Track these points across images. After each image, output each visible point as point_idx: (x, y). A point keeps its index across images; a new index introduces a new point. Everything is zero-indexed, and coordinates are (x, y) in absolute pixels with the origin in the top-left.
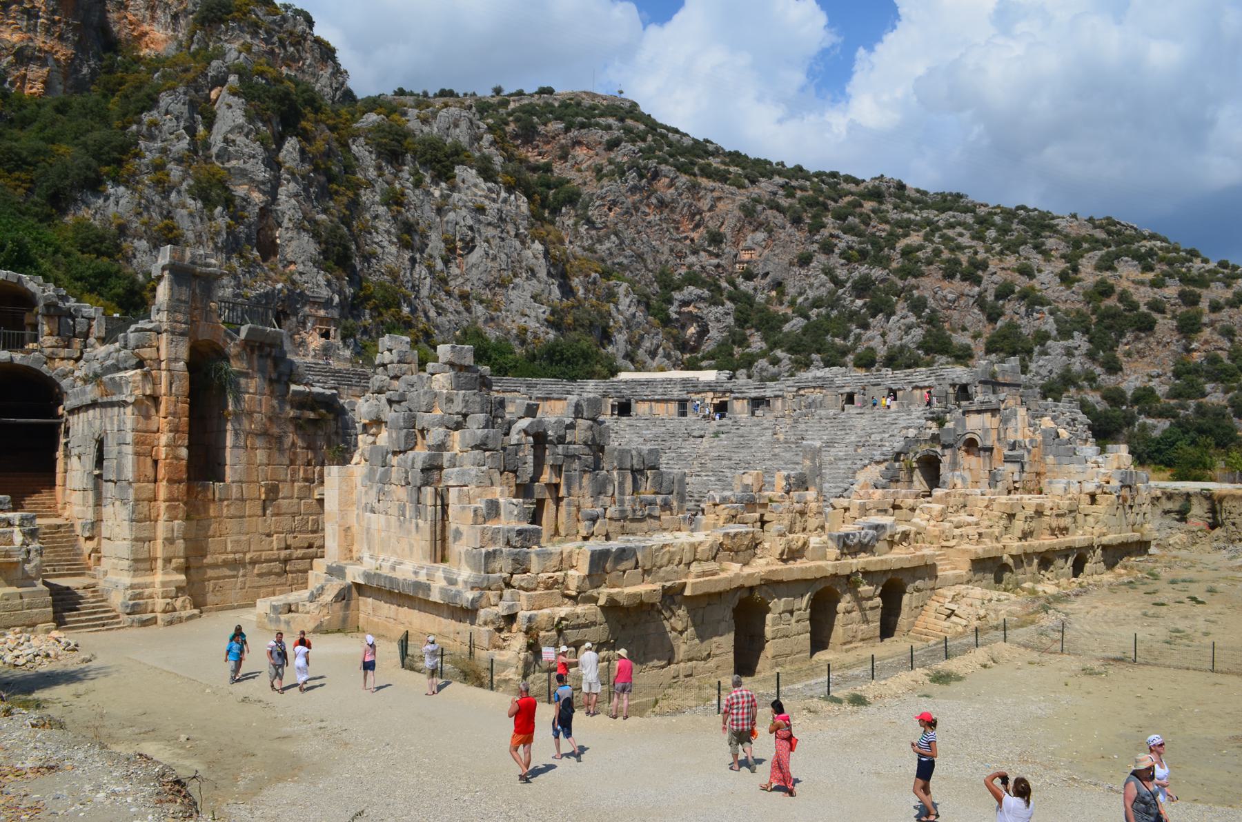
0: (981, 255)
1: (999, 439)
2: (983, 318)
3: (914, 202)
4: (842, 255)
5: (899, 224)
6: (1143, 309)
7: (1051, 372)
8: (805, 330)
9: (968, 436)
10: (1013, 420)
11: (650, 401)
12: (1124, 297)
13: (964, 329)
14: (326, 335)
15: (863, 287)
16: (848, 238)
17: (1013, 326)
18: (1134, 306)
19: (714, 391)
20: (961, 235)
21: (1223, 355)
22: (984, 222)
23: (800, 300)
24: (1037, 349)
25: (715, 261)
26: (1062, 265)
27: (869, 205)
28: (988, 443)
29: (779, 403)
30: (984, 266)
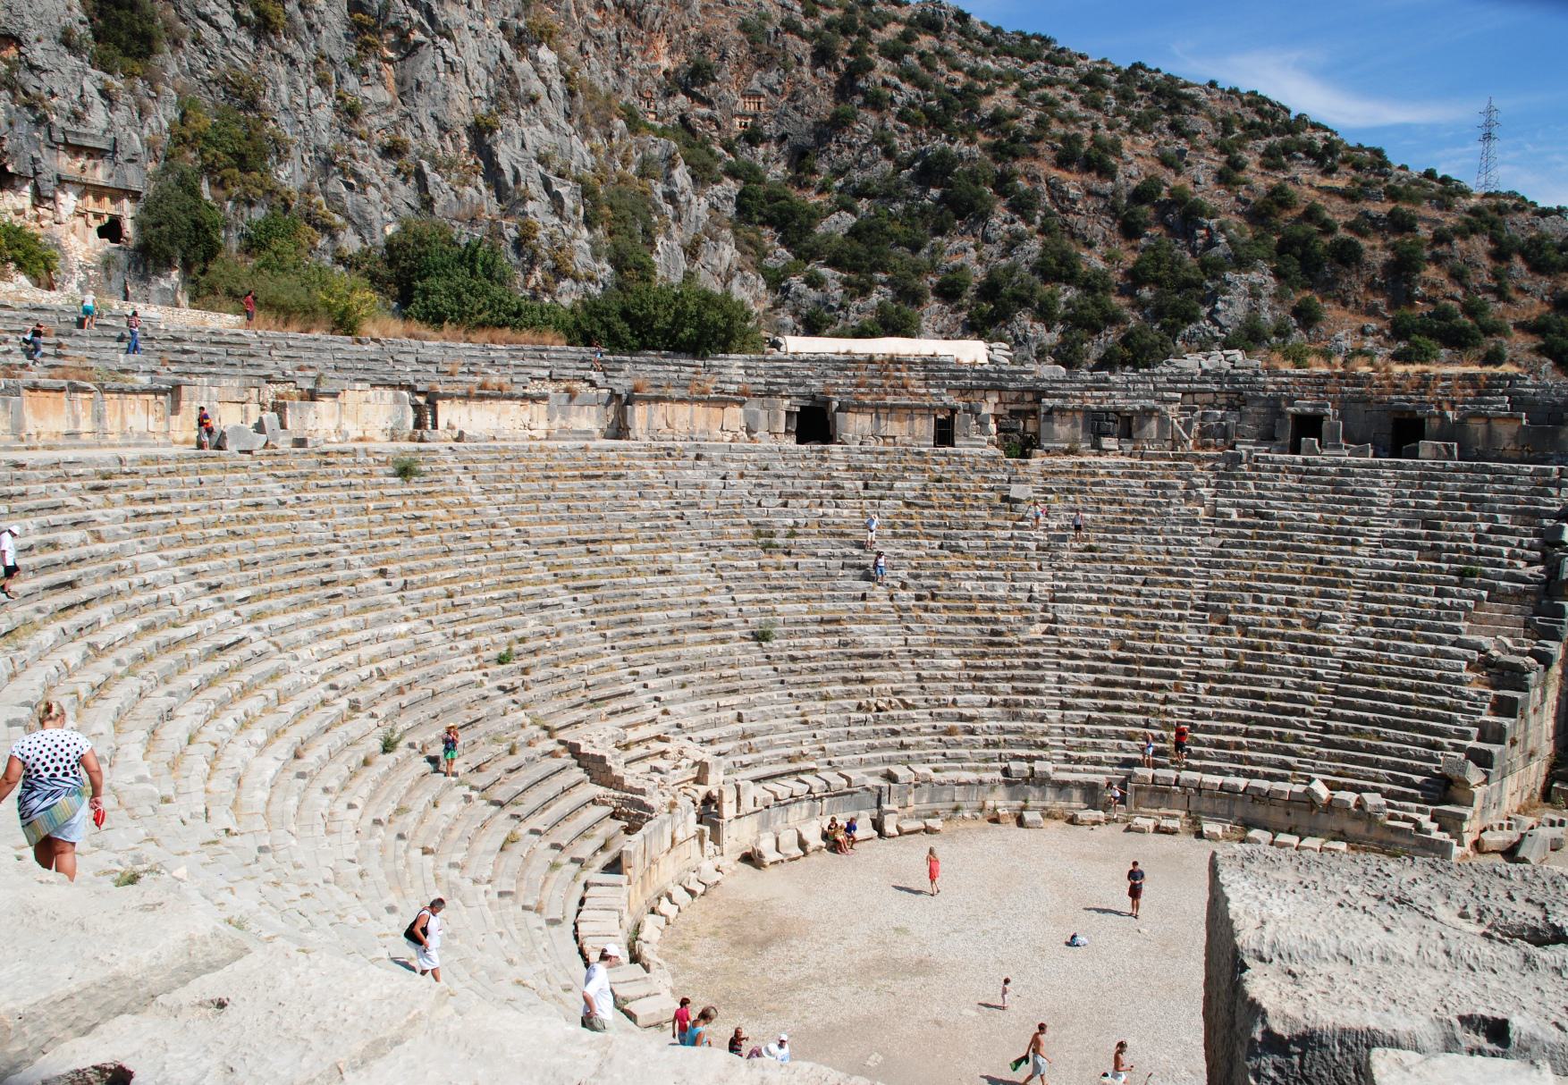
0: (1106, 134)
3: (987, 43)
4: (901, 116)
5: (972, 73)
6: (1342, 234)
8: (854, 232)
12: (1311, 214)
14: (111, 230)
15: (932, 170)
16: (905, 87)
18: (1328, 228)
20: (1066, 99)
22: (1093, 79)
23: (838, 184)
25: (705, 111)
26: (1219, 161)
27: (925, 42)
30: (1116, 148)
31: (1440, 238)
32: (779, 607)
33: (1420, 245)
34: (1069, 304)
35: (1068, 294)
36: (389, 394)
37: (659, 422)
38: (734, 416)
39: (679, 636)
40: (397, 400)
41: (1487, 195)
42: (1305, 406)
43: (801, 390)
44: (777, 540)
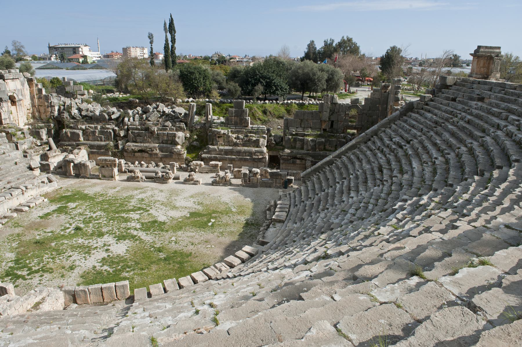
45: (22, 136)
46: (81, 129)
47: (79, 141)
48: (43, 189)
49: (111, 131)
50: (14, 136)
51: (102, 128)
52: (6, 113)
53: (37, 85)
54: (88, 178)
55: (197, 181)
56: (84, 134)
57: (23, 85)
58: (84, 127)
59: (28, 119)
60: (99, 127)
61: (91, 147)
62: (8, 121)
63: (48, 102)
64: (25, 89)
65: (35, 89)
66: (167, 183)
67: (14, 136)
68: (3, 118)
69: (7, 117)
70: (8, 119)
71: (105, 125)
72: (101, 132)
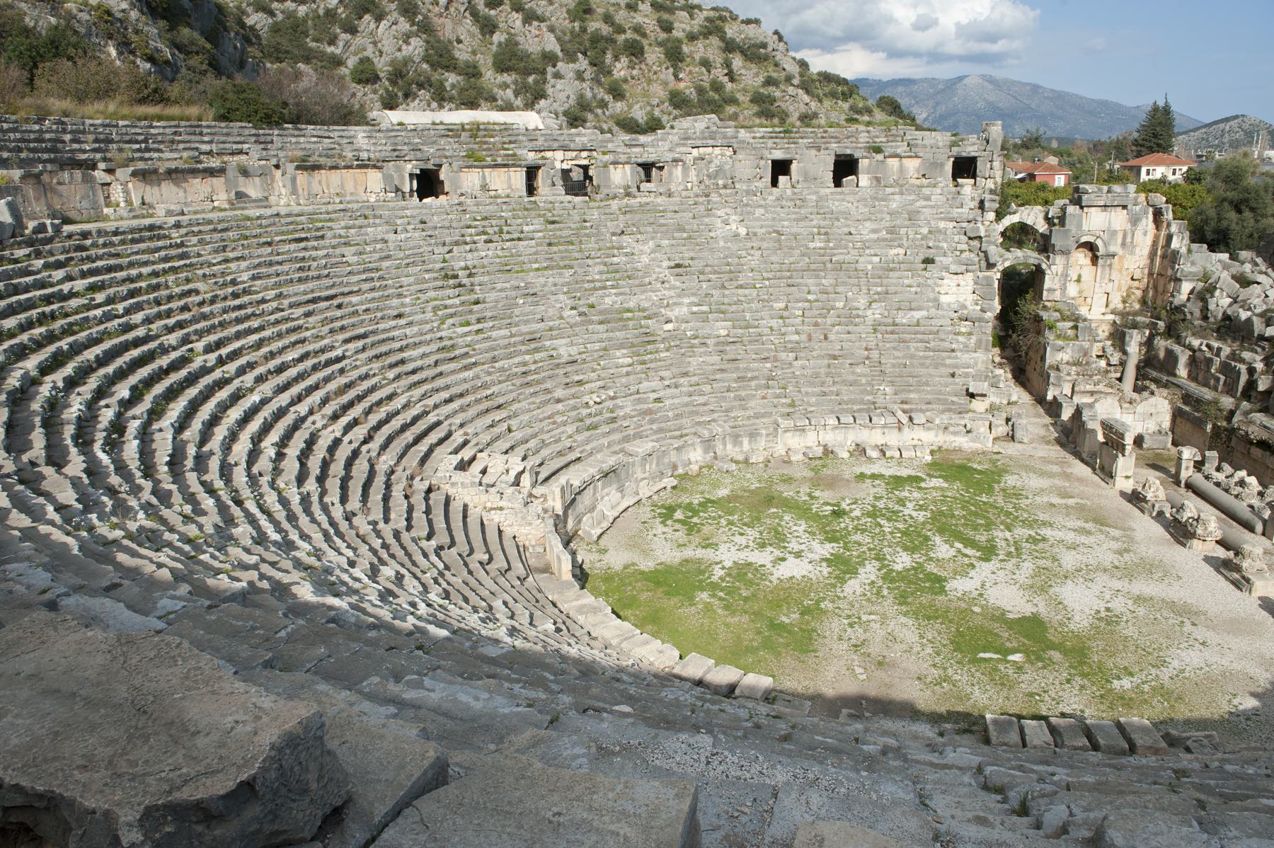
1: (1123, 244)
2: (475, 30)
6: (629, 35)
7: (568, 97)
9: (1083, 239)
10: (1144, 220)
11: (483, 167)
13: (459, 41)
17: (511, 43)
18: (621, 30)
19: (566, 149)
21: (707, 85)
24: (550, 70)
28: (1112, 249)
29: (678, 171)
31: (692, 38)
32: (494, 334)
33: (680, 41)
34: (453, 86)
35: (452, 79)
36: (78, 174)
37: (316, 188)
38: (374, 179)
39: (439, 369)
40: (88, 180)
41: (713, 9)
42: (779, 155)
43: (419, 155)
44: (465, 281)
45: (1070, 333)
46: (1190, 348)
47: (1175, 375)
48: (952, 438)
49: (1243, 368)
50: (1050, 328)
51: (1233, 356)
52: (1057, 279)
53: (1169, 225)
54: (1082, 461)
55: (1248, 581)
56: (1193, 362)
57: (1135, 221)
58: (1196, 343)
59: (1124, 302)
60: (1226, 350)
61: (1187, 398)
62: (1057, 295)
63: (1173, 268)
64: (1139, 234)
65: (1163, 233)
66: (1184, 545)
67: (1050, 328)
68: (1046, 286)
69: (1057, 287)
70: (1058, 293)
71: (1242, 348)
72: (1226, 368)
